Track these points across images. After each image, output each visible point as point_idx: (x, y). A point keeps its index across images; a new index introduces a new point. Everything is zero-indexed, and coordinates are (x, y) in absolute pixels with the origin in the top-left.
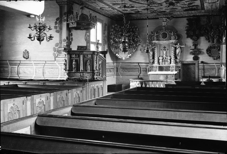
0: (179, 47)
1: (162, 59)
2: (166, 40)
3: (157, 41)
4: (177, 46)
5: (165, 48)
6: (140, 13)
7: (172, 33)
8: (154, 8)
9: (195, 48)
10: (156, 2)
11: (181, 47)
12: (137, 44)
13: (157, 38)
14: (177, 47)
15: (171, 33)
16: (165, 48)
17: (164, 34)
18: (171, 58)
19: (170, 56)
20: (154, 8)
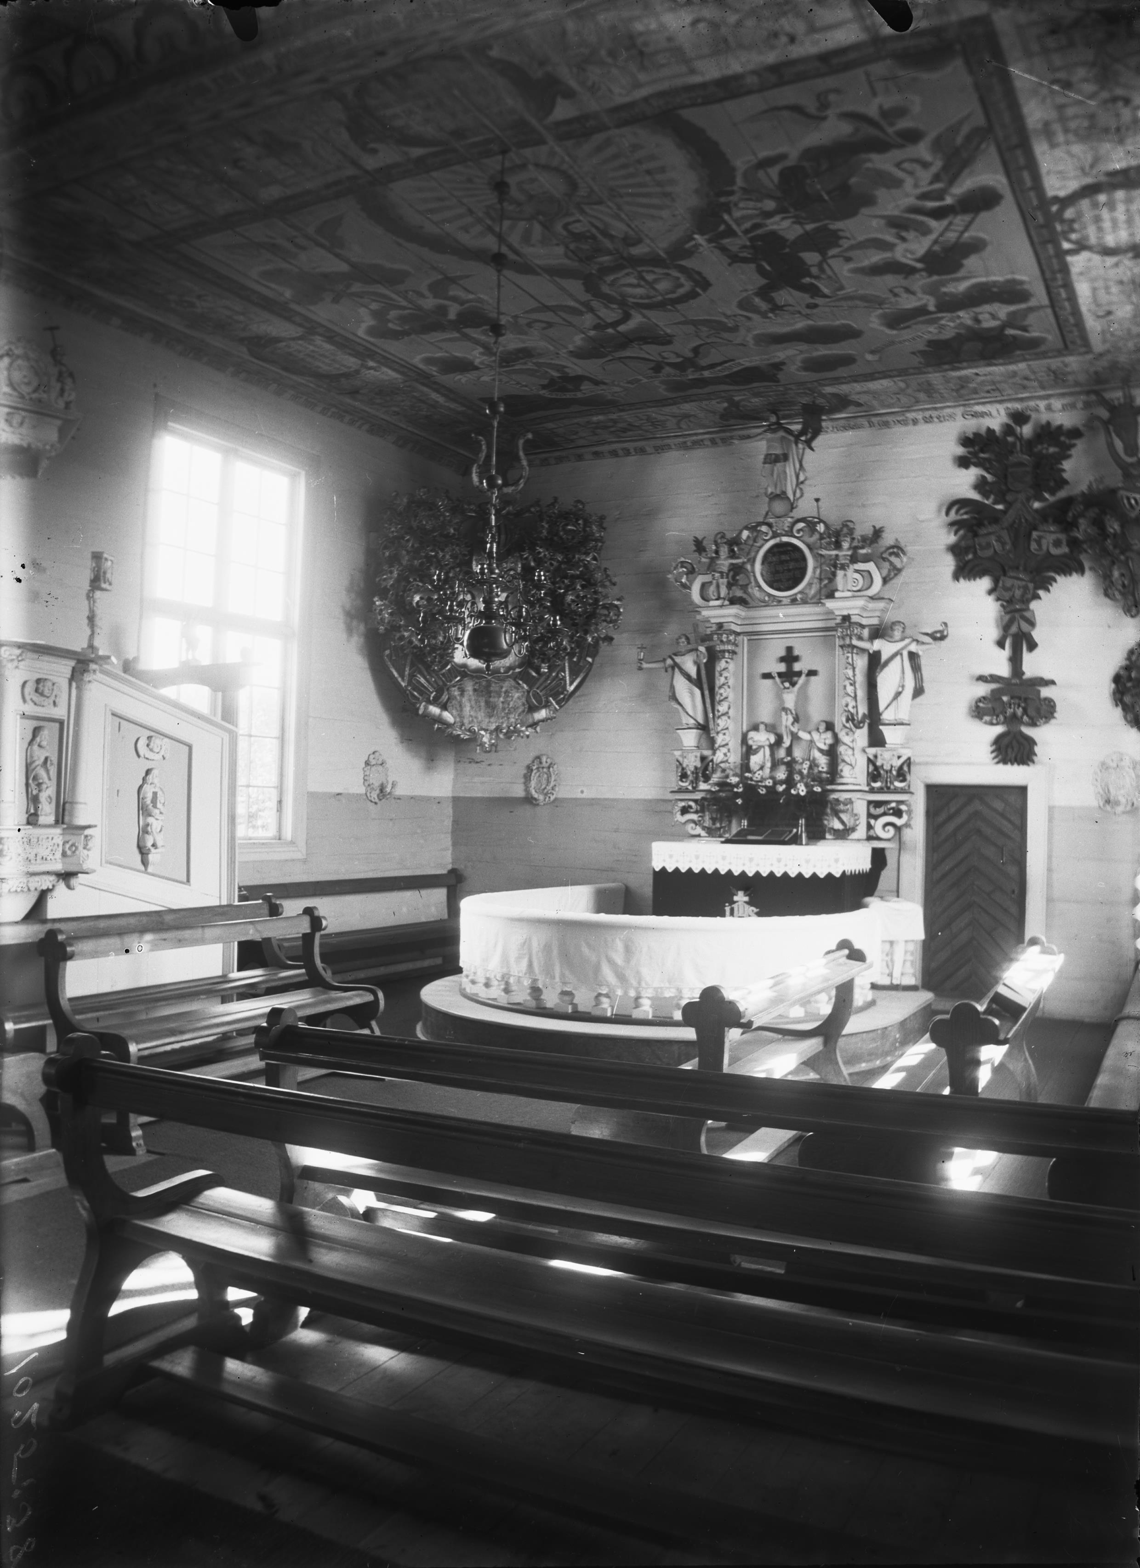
0: (898, 653)
1: (771, 746)
2: (794, 601)
3: (734, 610)
4: (886, 648)
5: (797, 659)
6: (587, 389)
7: (846, 545)
8: (662, 320)
9: (1016, 660)
10: (629, 242)
11: (913, 656)
12: (586, 632)
13: (729, 586)
14: (884, 657)
15: (838, 546)
16: (797, 659)
17: (784, 557)
18: (836, 736)
19: (830, 727)
20: (662, 320)
